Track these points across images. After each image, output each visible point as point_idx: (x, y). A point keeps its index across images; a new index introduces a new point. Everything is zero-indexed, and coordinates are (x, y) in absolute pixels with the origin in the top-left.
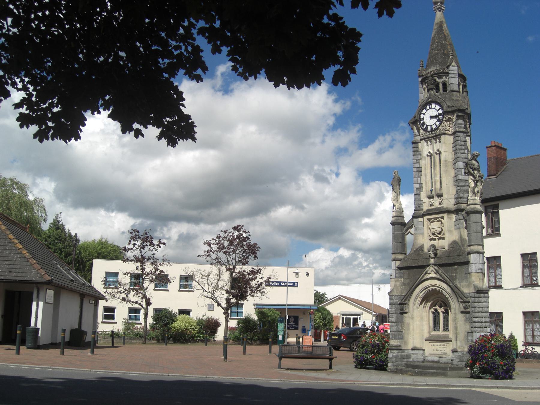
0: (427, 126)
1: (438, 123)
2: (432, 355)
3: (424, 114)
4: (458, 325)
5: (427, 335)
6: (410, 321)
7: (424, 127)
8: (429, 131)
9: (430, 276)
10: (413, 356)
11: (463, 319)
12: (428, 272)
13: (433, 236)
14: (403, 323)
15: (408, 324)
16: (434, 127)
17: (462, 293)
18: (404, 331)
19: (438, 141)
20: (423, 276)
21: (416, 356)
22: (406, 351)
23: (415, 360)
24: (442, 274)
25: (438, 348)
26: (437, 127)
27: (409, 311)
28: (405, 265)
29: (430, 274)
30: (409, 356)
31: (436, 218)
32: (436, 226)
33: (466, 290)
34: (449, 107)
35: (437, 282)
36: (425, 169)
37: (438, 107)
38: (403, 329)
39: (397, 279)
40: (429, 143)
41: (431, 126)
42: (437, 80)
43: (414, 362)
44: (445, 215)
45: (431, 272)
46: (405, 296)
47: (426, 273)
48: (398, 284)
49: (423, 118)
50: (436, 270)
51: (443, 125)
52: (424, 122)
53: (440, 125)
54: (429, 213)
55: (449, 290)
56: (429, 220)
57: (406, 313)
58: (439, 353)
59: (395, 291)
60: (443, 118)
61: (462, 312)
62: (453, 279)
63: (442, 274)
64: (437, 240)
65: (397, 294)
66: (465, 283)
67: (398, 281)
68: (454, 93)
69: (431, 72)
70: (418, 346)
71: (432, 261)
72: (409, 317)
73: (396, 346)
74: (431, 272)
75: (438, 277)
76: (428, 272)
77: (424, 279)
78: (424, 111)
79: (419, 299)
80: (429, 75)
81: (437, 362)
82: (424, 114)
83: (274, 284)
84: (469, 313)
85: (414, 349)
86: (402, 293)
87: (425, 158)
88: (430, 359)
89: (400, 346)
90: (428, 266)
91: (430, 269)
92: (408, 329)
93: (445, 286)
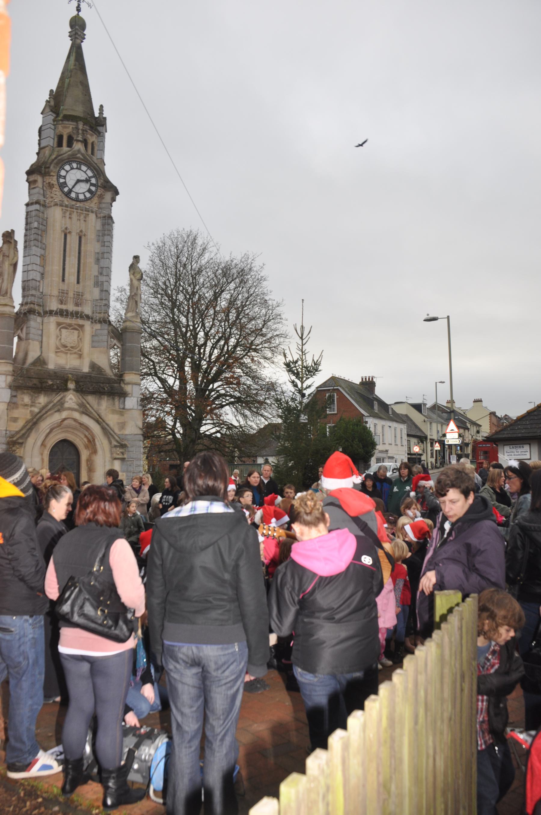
1: (88, 195)
3: (67, 172)
7: (66, 189)
8: (72, 199)
13: (63, 349)
26: (86, 200)
32: (69, 337)
44: (87, 324)
52: (65, 183)
53: (90, 199)
60: (97, 190)
82: (67, 172)
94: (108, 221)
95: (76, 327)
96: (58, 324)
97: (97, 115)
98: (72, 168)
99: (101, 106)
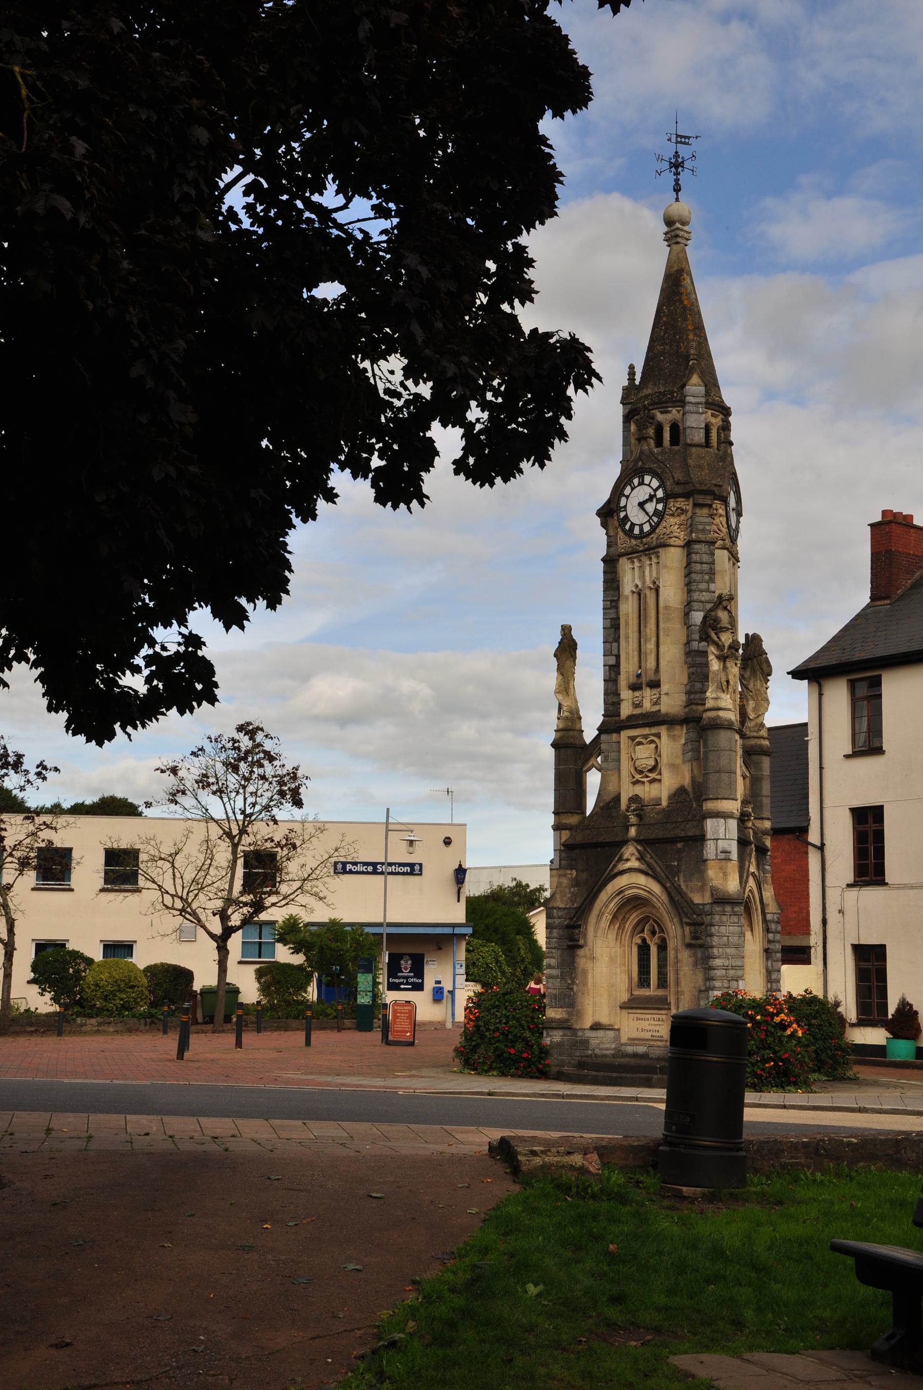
0: (633, 525)
2: (633, 1041)
4: (681, 974)
5: (625, 997)
6: (589, 965)
7: (627, 527)
9: (628, 865)
10: (593, 1043)
11: (691, 960)
12: (625, 857)
13: (638, 777)
14: (574, 969)
15: (585, 972)
16: (647, 528)
17: (690, 903)
18: (575, 988)
19: (654, 560)
20: (615, 866)
21: (602, 1043)
22: (580, 1034)
23: (598, 1052)
24: (651, 861)
25: (645, 1025)
27: (585, 942)
28: (579, 839)
29: (628, 860)
30: (585, 1043)
31: (645, 737)
32: (644, 755)
33: (697, 899)
34: (678, 483)
35: (642, 880)
36: (627, 623)
37: (655, 483)
38: (573, 983)
39: (562, 872)
40: (637, 564)
41: (641, 526)
42: (660, 417)
43: (596, 1056)
44: (663, 730)
45: (631, 857)
46: (578, 909)
47: (620, 859)
48: (565, 881)
49: (625, 507)
50: (639, 851)
51: (664, 524)
52: (626, 516)
53: (658, 524)
54: (633, 722)
55: (664, 898)
56: (633, 738)
57: (581, 947)
58: (648, 1035)
59: (558, 896)
60: (665, 508)
61: (689, 946)
62: (673, 872)
63: (651, 861)
64: (647, 784)
65: (562, 906)
66: (695, 883)
67: (565, 875)
68: (694, 450)
69: (646, 396)
70: (604, 1020)
71: (633, 832)
72: (585, 956)
73: (560, 1021)
74: (631, 857)
75: (643, 867)
76: (625, 857)
77: (615, 871)
79: (607, 917)
80: (640, 405)
81: (645, 1056)
82: (627, 497)
83: (360, 868)
84: (701, 946)
85: (596, 1027)
86: (573, 902)
87: (627, 598)
88: (630, 1049)
89: (567, 1021)
90: (625, 842)
91: (630, 851)
92: (585, 984)
93: (656, 888)
95: (652, 738)
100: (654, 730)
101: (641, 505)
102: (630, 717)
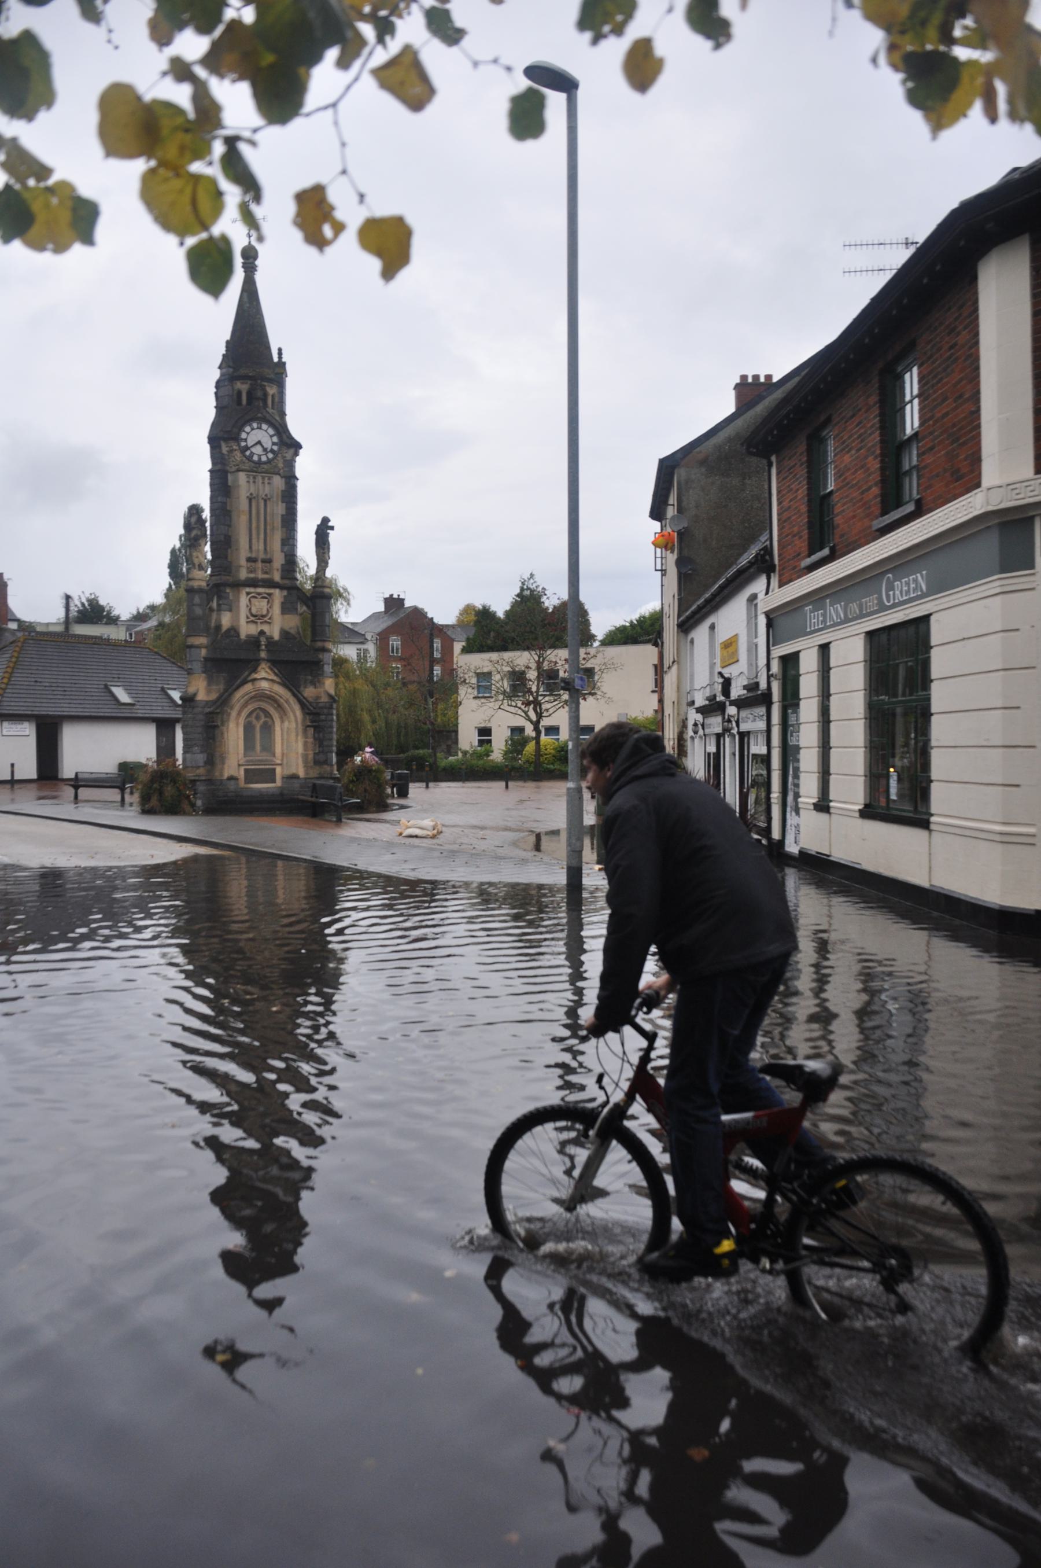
1: (270, 456)
7: (248, 453)
8: (254, 462)
13: (252, 618)
26: (269, 461)
37: (271, 431)
44: (277, 592)
45: (264, 672)
56: (248, 594)
60: (279, 449)
71: (263, 655)
74: (264, 672)
78: (248, 429)
94: (291, 480)
96: (248, 594)
97: (276, 359)
98: (253, 429)
99: (280, 350)
100: (268, 591)
101: (259, 443)
102: (248, 579)
